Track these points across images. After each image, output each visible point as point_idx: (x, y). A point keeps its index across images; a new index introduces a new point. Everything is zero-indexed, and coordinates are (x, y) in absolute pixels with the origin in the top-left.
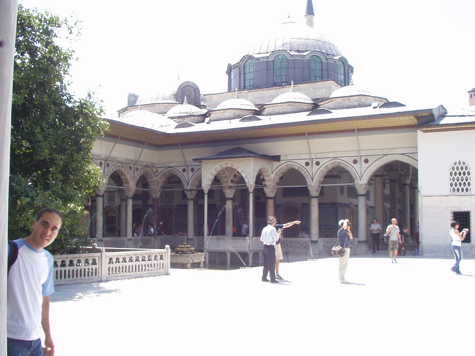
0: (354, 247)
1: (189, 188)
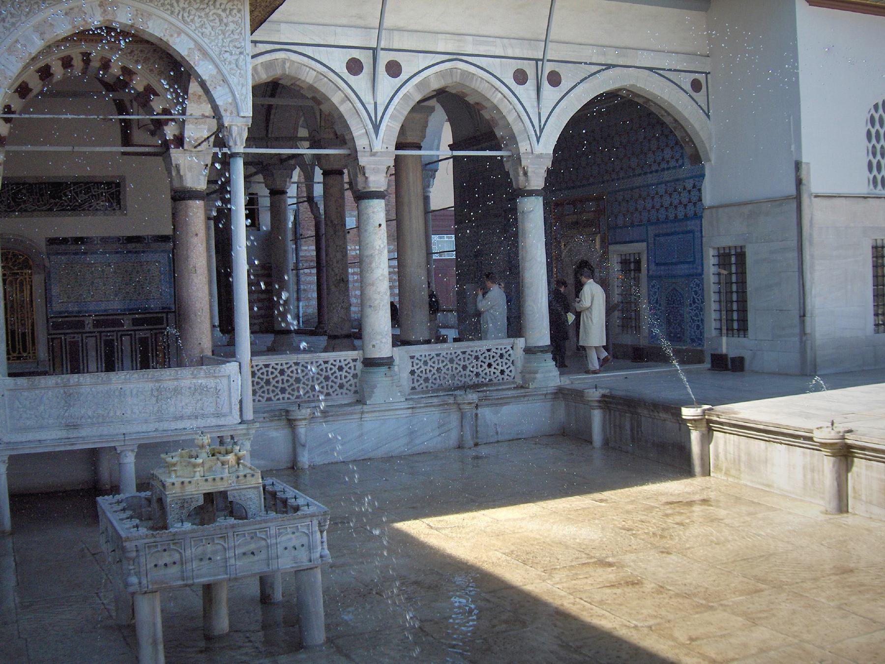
0: (512, 368)
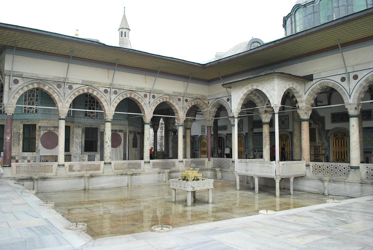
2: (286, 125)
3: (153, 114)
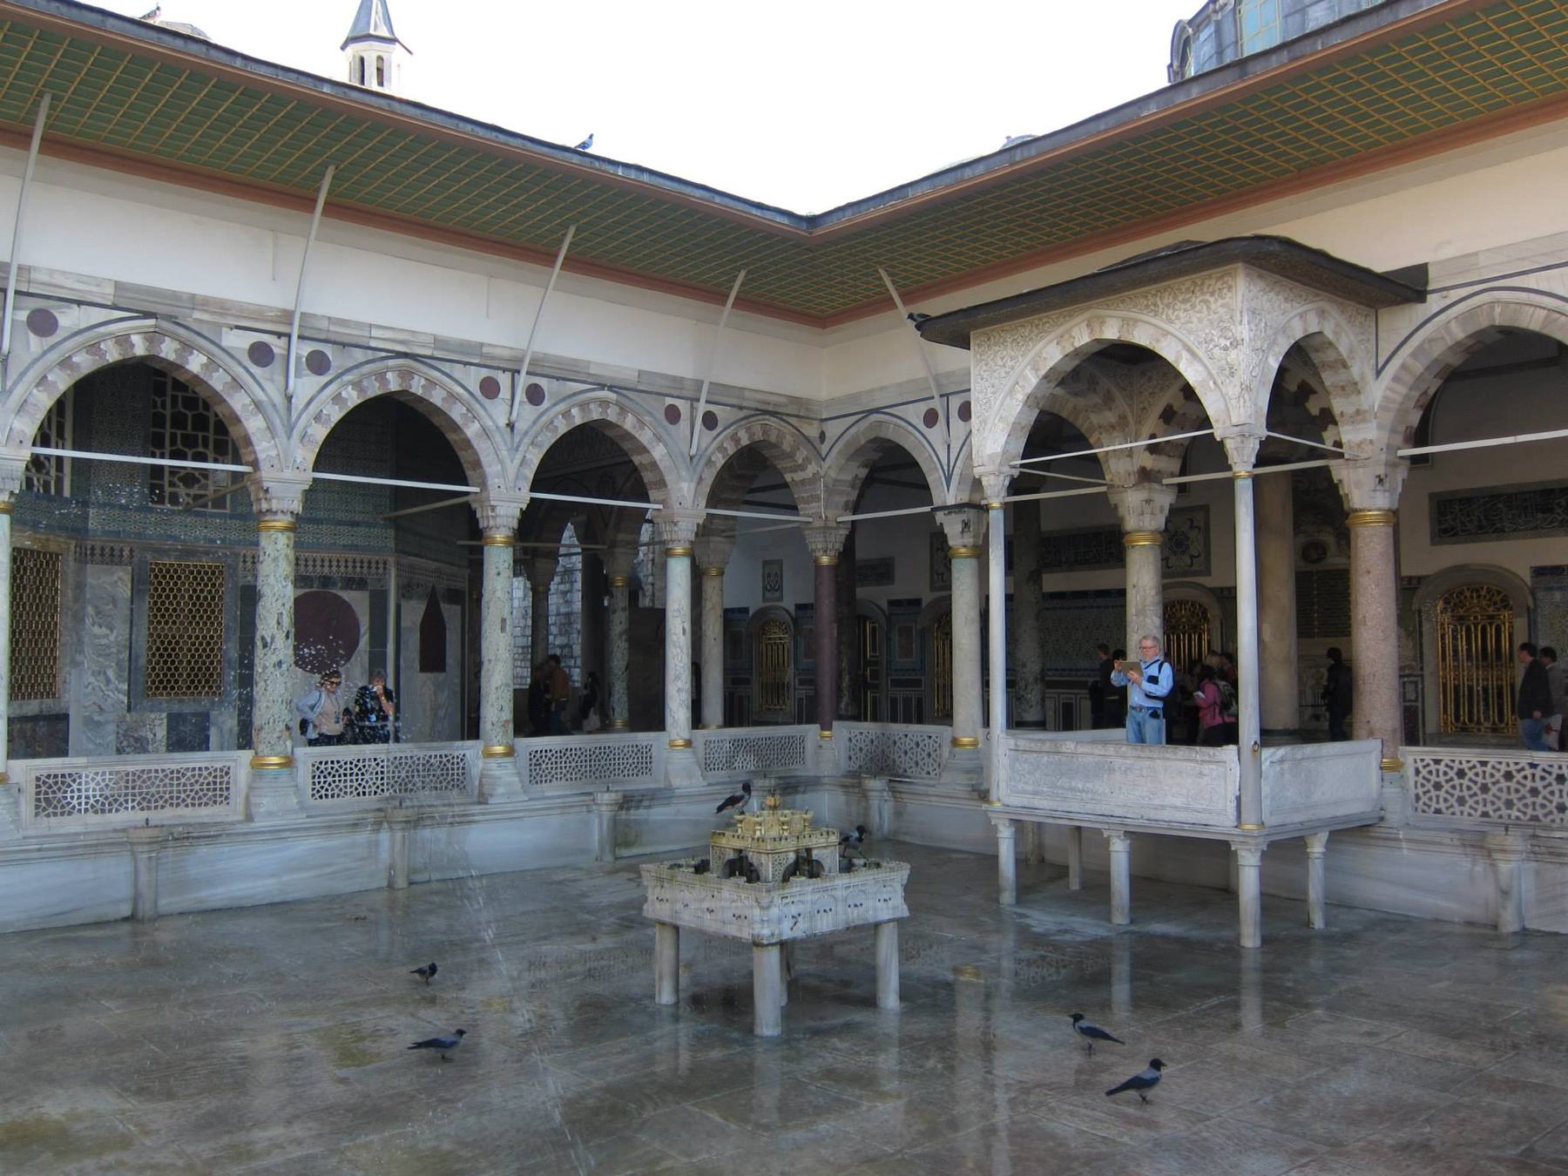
1: (951, 501)
2: (1192, 557)
3: (532, 490)
